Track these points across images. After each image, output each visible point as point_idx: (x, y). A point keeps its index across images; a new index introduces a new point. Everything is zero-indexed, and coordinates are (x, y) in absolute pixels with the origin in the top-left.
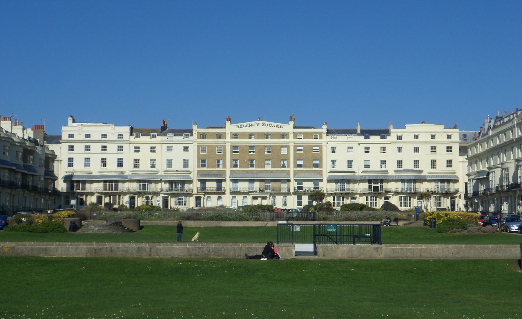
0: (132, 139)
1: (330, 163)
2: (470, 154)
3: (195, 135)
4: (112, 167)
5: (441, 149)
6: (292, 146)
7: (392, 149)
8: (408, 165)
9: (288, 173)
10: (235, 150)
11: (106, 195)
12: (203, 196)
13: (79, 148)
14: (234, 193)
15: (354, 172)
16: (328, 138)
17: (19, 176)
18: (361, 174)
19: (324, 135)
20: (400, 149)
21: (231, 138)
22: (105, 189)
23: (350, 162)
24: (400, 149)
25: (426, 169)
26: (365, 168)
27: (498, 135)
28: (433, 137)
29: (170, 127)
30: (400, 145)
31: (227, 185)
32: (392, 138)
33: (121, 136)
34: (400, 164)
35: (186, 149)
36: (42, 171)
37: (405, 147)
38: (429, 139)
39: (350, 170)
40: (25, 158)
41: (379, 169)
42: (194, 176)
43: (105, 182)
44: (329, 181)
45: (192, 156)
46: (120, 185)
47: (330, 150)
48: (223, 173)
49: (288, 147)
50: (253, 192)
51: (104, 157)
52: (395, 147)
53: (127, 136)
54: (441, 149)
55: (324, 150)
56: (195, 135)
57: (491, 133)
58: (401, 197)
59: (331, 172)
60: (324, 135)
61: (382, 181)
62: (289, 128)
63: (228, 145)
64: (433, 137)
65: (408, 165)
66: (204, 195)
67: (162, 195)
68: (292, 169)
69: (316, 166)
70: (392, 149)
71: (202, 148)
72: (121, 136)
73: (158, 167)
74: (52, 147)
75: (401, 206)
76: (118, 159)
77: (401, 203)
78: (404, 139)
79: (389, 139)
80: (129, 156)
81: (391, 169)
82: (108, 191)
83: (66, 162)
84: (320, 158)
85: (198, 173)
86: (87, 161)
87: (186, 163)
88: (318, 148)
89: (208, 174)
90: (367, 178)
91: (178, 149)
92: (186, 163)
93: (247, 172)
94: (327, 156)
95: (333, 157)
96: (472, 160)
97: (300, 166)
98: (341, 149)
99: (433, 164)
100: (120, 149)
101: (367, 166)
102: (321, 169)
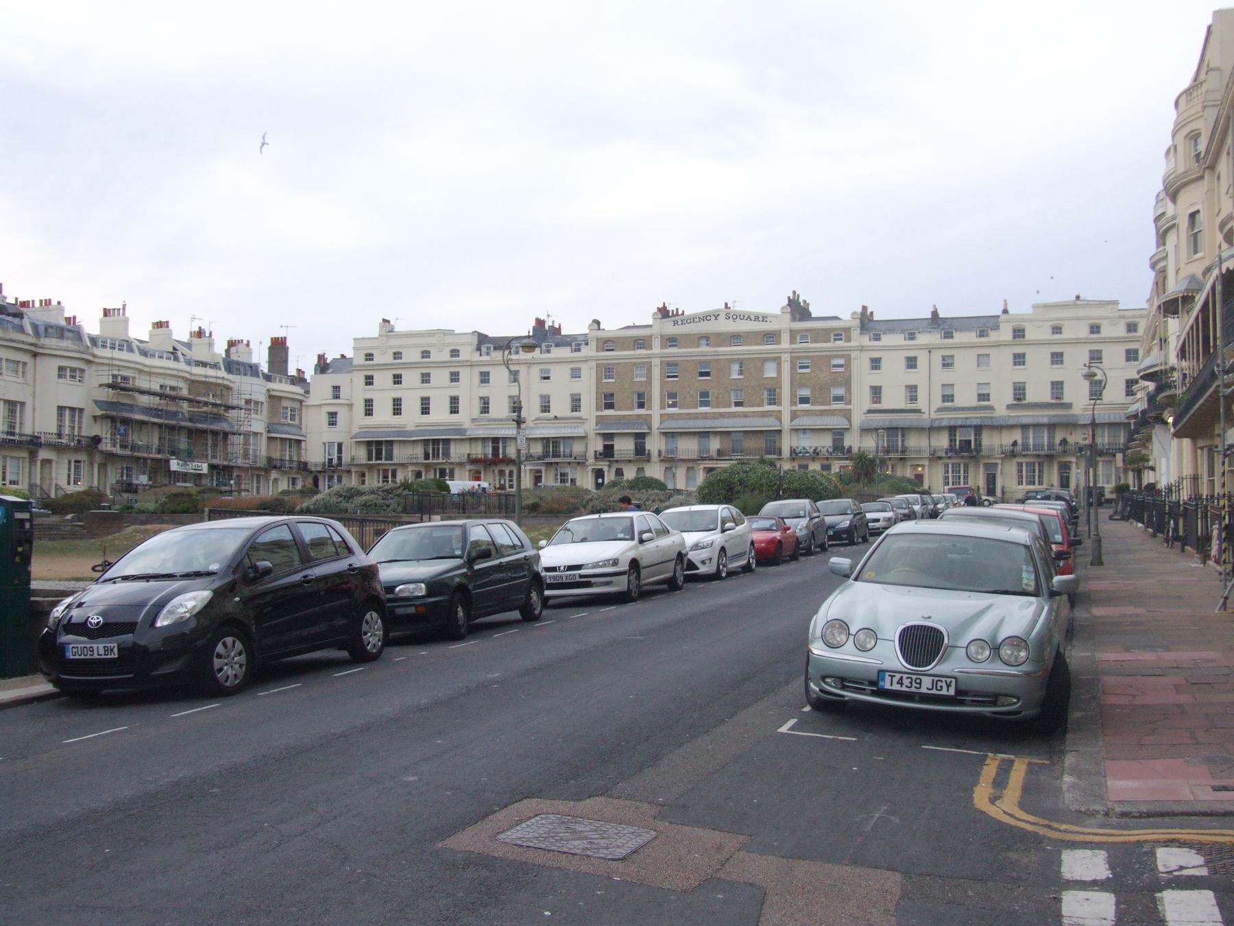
0: (476, 357)
1: (867, 394)
4: (440, 415)
6: (786, 357)
8: (1038, 392)
9: (778, 416)
10: (671, 370)
11: (428, 467)
12: (606, 469)
14: (670, 461)
15: (919, 411)
16: (865, 340)
18: (933, 416)
19: (855, 334)
20: (1019, 359)
21: (663, 346)
22: (427, 456)
23: (912, 390)
24: (1019, 359)
26: (944, 401)
28: (1095, 329)
30: (1019, 350)
31: (654, 445)
34: (1019, 391)
35: (576, 374)
37: (1031, 354)
38: (1084, 332)
39: (913, 406)
41: (974, 402)
42: (590, 428)
43: (426, 442)
44: (865, 431)
45: (587, 387)
46: (396, 451)
47: (867, 364)
48: (647, 420)
49: (777, 360)
50: (703, 459)
51: (425, 394)
52: (1007, 355)
55: (855, 365)
58: (1020, 465)
59: (870, 411)
60: (855, 334)
61: (978, 429)
63: (656, 362)
64: (1095, 329)
65: (1038, 392)
66: (609, 466)
67: (411, 468)
68: (786, 408)
69: (838, 399)
71: (606, 370)
75: (1020, 483)
76: (422, 399)
77: (1021, 477)
78: (1029, 336)
79: (994, 336)
80: (468, 390)
81: (1001, 400)
82: (373, 462)
83: (360, 407)
84: (847, 383)
85: (600, 420)
86: (397, 408)
87: (576, 404)
88: (841, 362)
89: (619, 421)
90: (945, 423)
91: (560, 374)
92: (576, 404)
93: (696, 417)
95: (876, 379)
97: (804, 400)
100: (455, 377)
101: (948, 398)
102: (848, 407)
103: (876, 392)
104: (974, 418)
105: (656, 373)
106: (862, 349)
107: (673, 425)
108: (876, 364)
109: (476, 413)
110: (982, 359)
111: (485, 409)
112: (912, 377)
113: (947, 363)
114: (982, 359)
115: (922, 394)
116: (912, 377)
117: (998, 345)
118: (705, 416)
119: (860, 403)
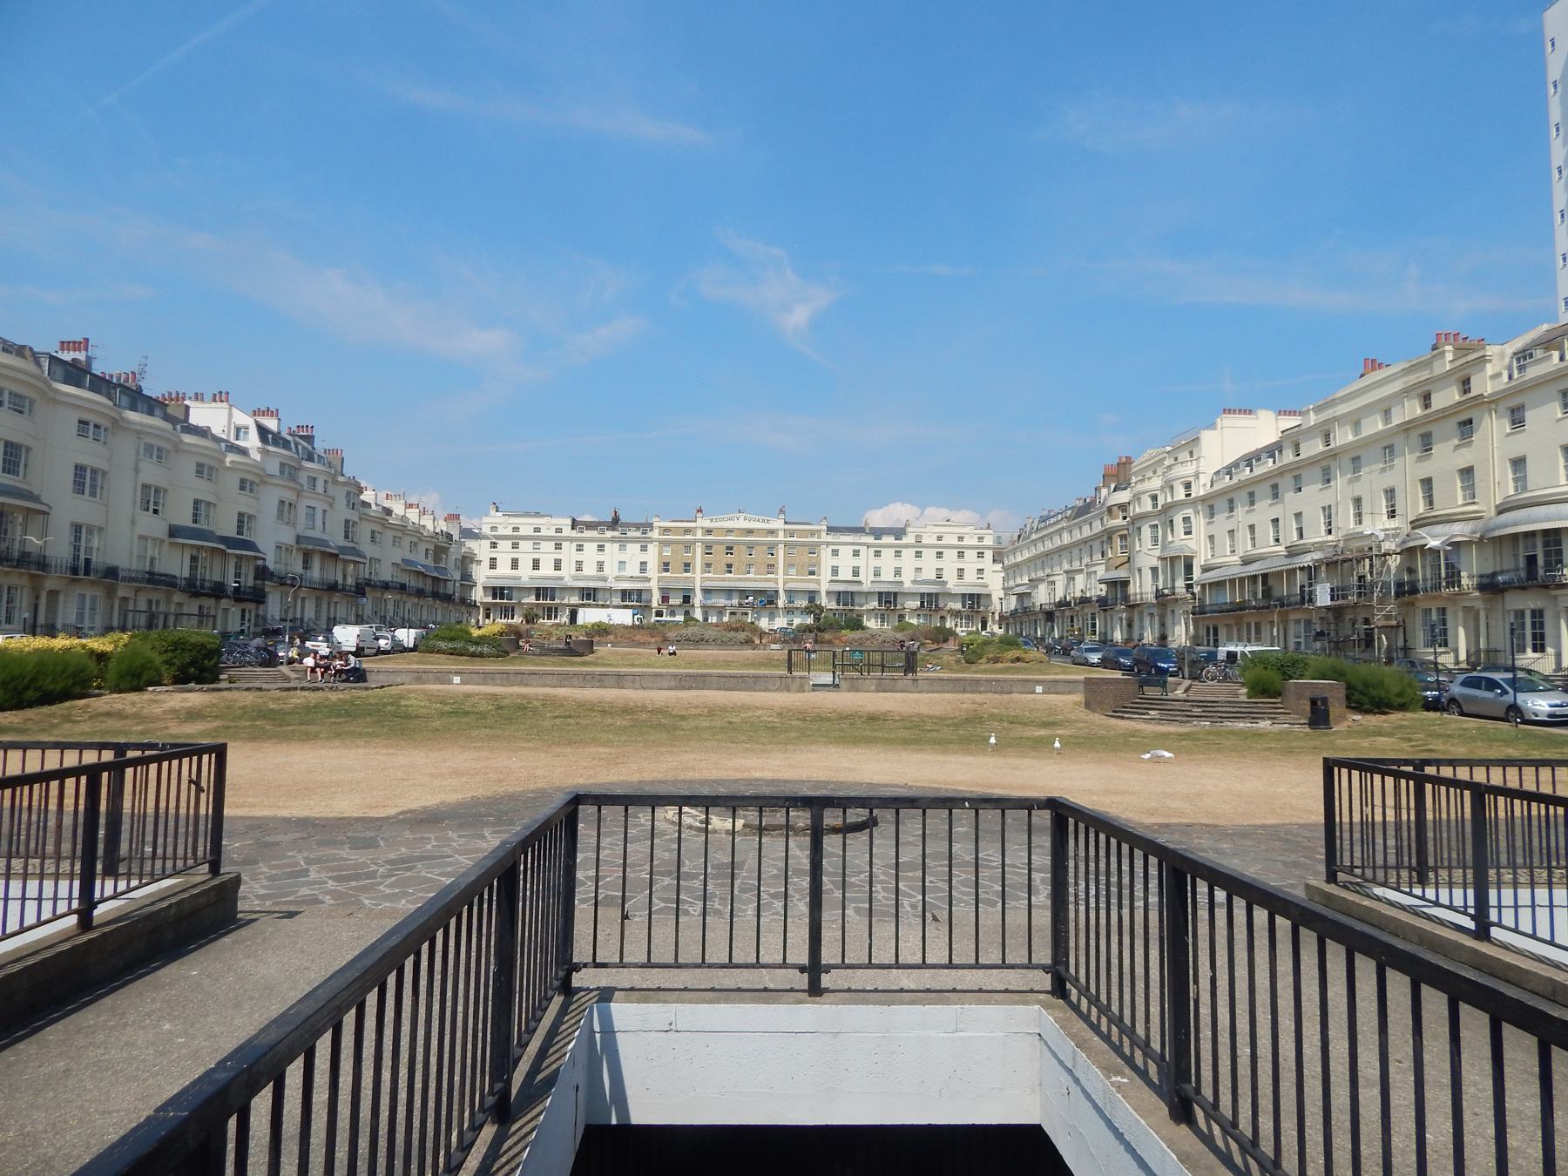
0: (574, 534)
2: (1010, 560)
3: (656, 531)
4: (547, 570)
5: (971, 555)
7: (908, 554)
9: (776, 581)
13: (505, 545)
17: (429, 581)
24: (918, 554)
25: (950, 578)
27: (1042, 539)
29: (623, 519)
31: (698, 599)
32: (909, 539)
33: (559, 530)
35: (644, 549)
36: (457, 576)
40: (437, 559)
42: (654, 585)
45: (652, 556)
53: (567, 531)
54: (971, 555)
56: (656, 531)
57: (1034, 537)
60: (824, 534)
62: (778, 524)
68: (781, 576)
70: (908, 554)
72: (559, 530)
73: (607, 571)
74: (472, 544)
79: (905, 540)
83: (486, 563)
86: (515, 564)
93: (724, 580)
94: (826, 560)
96: (1011, 571)
98: (846, 552)
99: (961, 571)
103: (835, 571)
104: (893, 589)
105: (699, 549)
106: (828, 544)
107: (708, 584)
108: (835, 553)
109: (573, 572)
110: (898, 554)
111: (579, 569)
112: (856, 562)
113: (877, 554)
114: (898, 554)
115: (862, 572)
116: (856, 562)
117: (906, 546)
118: (730, 580)
119: (825, 576)
